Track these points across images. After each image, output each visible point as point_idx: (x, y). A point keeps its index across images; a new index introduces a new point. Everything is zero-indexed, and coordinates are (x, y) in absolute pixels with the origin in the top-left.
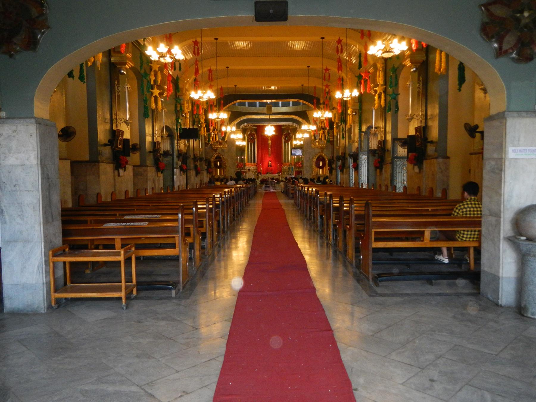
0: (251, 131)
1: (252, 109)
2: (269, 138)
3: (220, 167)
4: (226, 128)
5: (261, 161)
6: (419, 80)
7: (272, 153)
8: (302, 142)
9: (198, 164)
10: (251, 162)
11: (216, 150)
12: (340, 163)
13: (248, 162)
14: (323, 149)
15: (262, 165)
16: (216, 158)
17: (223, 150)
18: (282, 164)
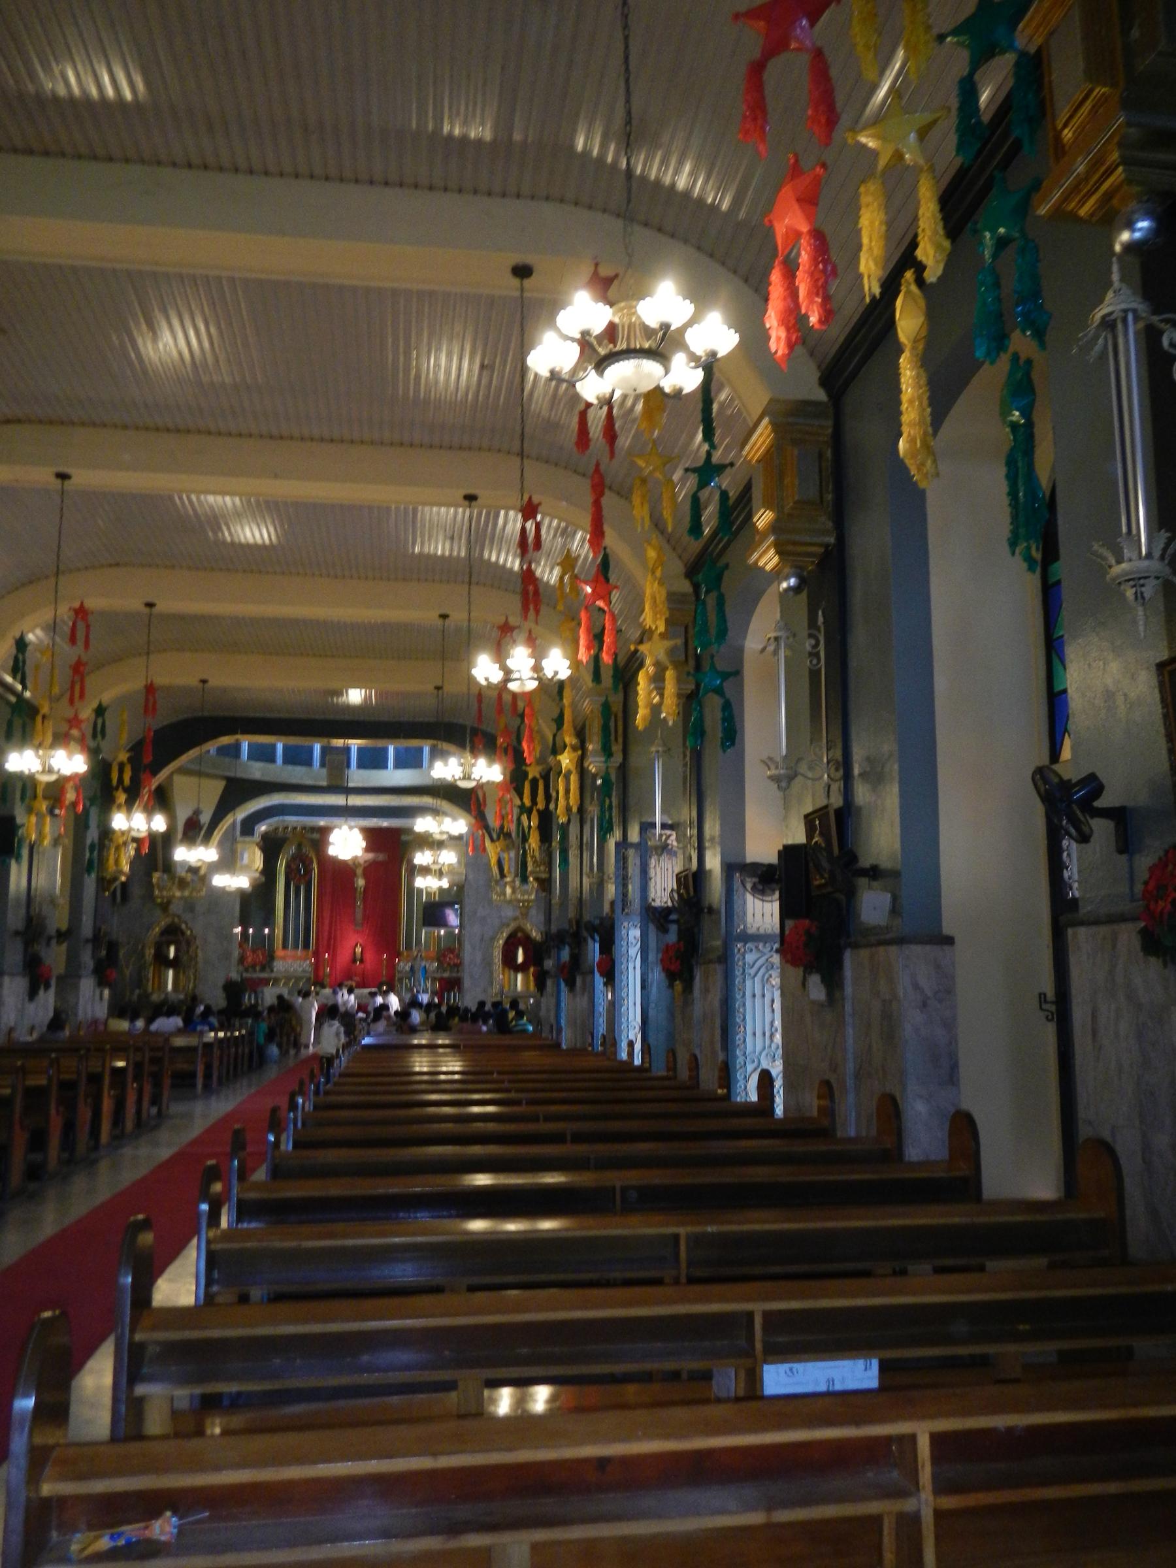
0: (299, 846)
1: (297, 774)
2: (359, 871)
3: (175, 964)
4: (129, 818)
5: (332, 947)
6: (812, 623)
7: (366, 918)
8: (445, 883)
9: (55, 957)
10: (296, 947)
11: (165, 907)
12: (565, 955)
13: (285, 946)
14: (528, 908)
15: (333, 956)
16: (162, 933)
17: (190, 906)
18: (399, 955)
